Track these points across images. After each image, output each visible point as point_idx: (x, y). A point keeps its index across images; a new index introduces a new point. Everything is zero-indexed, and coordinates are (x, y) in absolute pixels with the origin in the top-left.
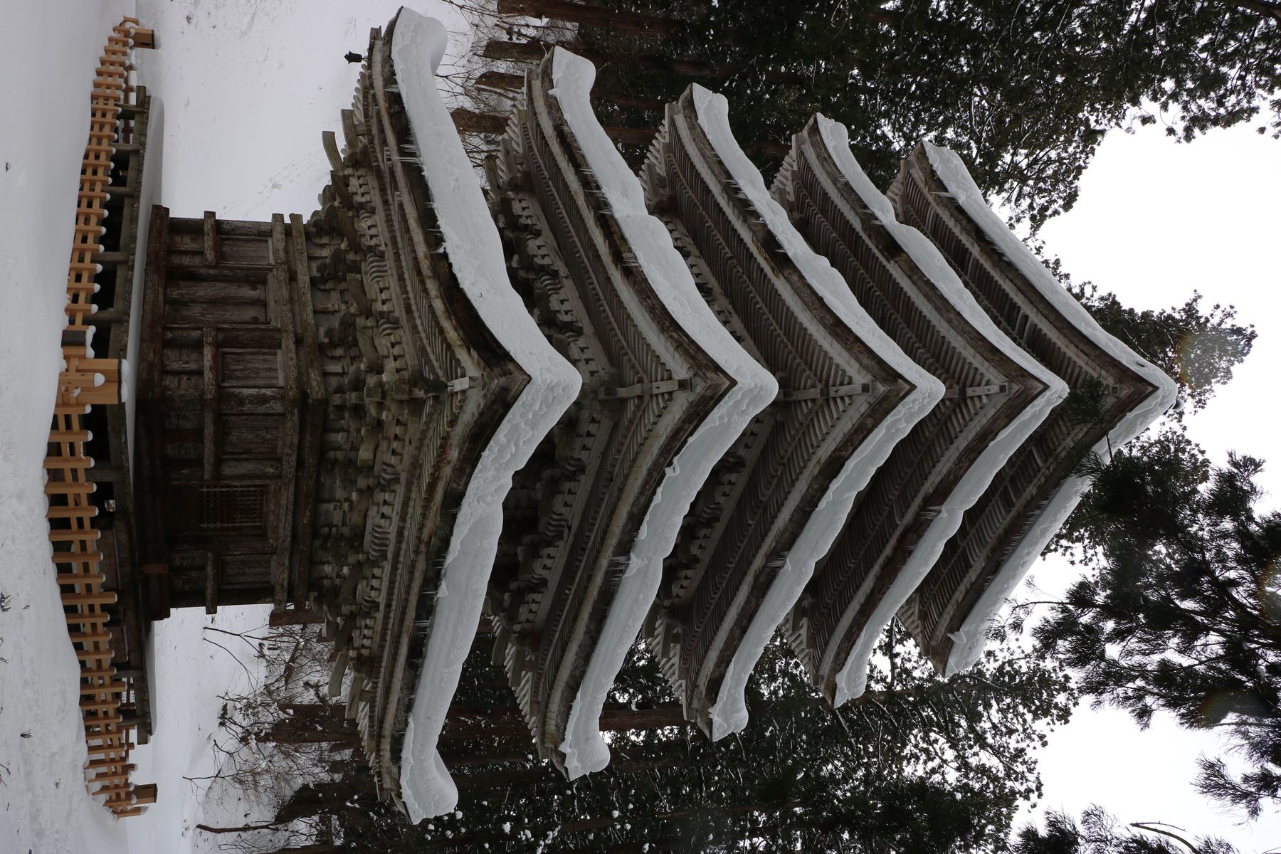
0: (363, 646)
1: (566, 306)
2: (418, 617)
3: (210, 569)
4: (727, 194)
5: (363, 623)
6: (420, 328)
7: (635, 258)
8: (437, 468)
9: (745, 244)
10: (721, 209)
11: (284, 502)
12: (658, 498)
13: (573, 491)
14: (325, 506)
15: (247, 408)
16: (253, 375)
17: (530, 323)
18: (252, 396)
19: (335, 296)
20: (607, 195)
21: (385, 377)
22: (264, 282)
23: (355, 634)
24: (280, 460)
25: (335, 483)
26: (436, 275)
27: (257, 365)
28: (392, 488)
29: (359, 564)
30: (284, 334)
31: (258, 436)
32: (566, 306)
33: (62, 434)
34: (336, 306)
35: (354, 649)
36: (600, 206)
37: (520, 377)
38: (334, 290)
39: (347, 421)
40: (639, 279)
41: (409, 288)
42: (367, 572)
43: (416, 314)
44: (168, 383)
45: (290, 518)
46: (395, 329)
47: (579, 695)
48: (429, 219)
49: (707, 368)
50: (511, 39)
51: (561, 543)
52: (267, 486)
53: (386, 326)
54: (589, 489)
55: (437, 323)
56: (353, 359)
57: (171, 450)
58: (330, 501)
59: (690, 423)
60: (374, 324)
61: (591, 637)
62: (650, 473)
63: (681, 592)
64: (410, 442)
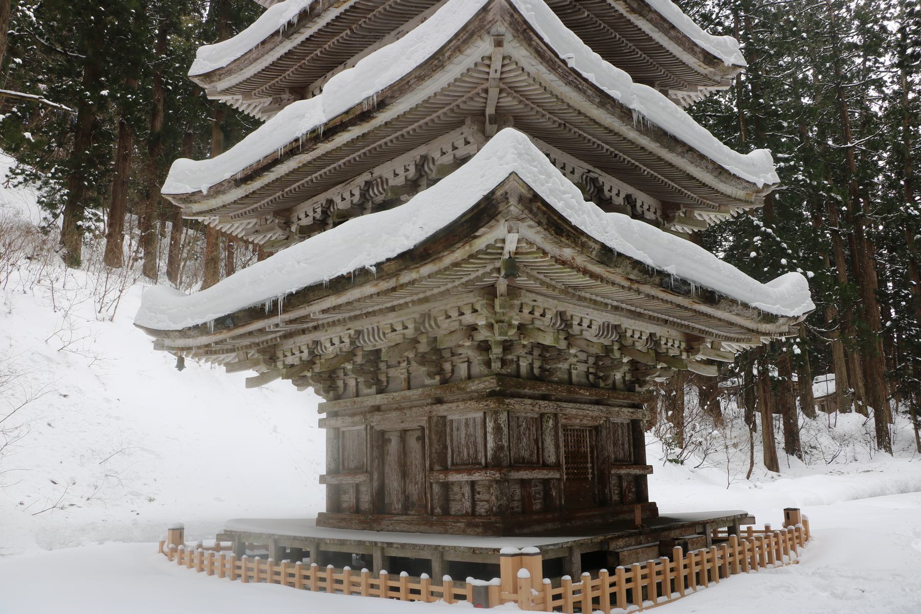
0: (679, 347)
1: (401, 172)
2: (687, 294)
3: (623, 472)
4: (293, 34)
5: (664, 346)
6: (443, 289)
7: (368, 98)
9: (341, 13)
10: (307, 39)
11: (574, 412)
12: (591, 77)
13: (562, 165)
14: (574, 378)
16: (472, 439)
17: (423, 197)
18: (495, 439)
19: (392, 372)
20: (304, 131)
21: (481, 322)
22: (383, 433)
23: (672, 353)
25: (560, 369)
26: (396, 274)
27: (463, 436)
28: (569, 318)
29: (622, 348)
30: (434, 413)
31: (524, 434)
32: (401, 172)
33: (566, 602)
34: (403, 371)
35: (681, 355)
36: (316, 136)
37: (512, 183)
38: (387, 374)
40: (389, 93)
41: (402, 301)
42: (629, 342)
43: (428, 293)
44: (483, 510)
45: (586, 406)
47: (726, 167)
48: (340, 284)
50: (141, 258)
51: (601, 180)
53: (427, 325)
54: (560, 151)
55: (446, 269)
57: (537, 506)
58: (570, 373)
59: (531, 39)
60: (424, 336)
61: (687, 151)
62: (569, 83)
64: (535, 301)
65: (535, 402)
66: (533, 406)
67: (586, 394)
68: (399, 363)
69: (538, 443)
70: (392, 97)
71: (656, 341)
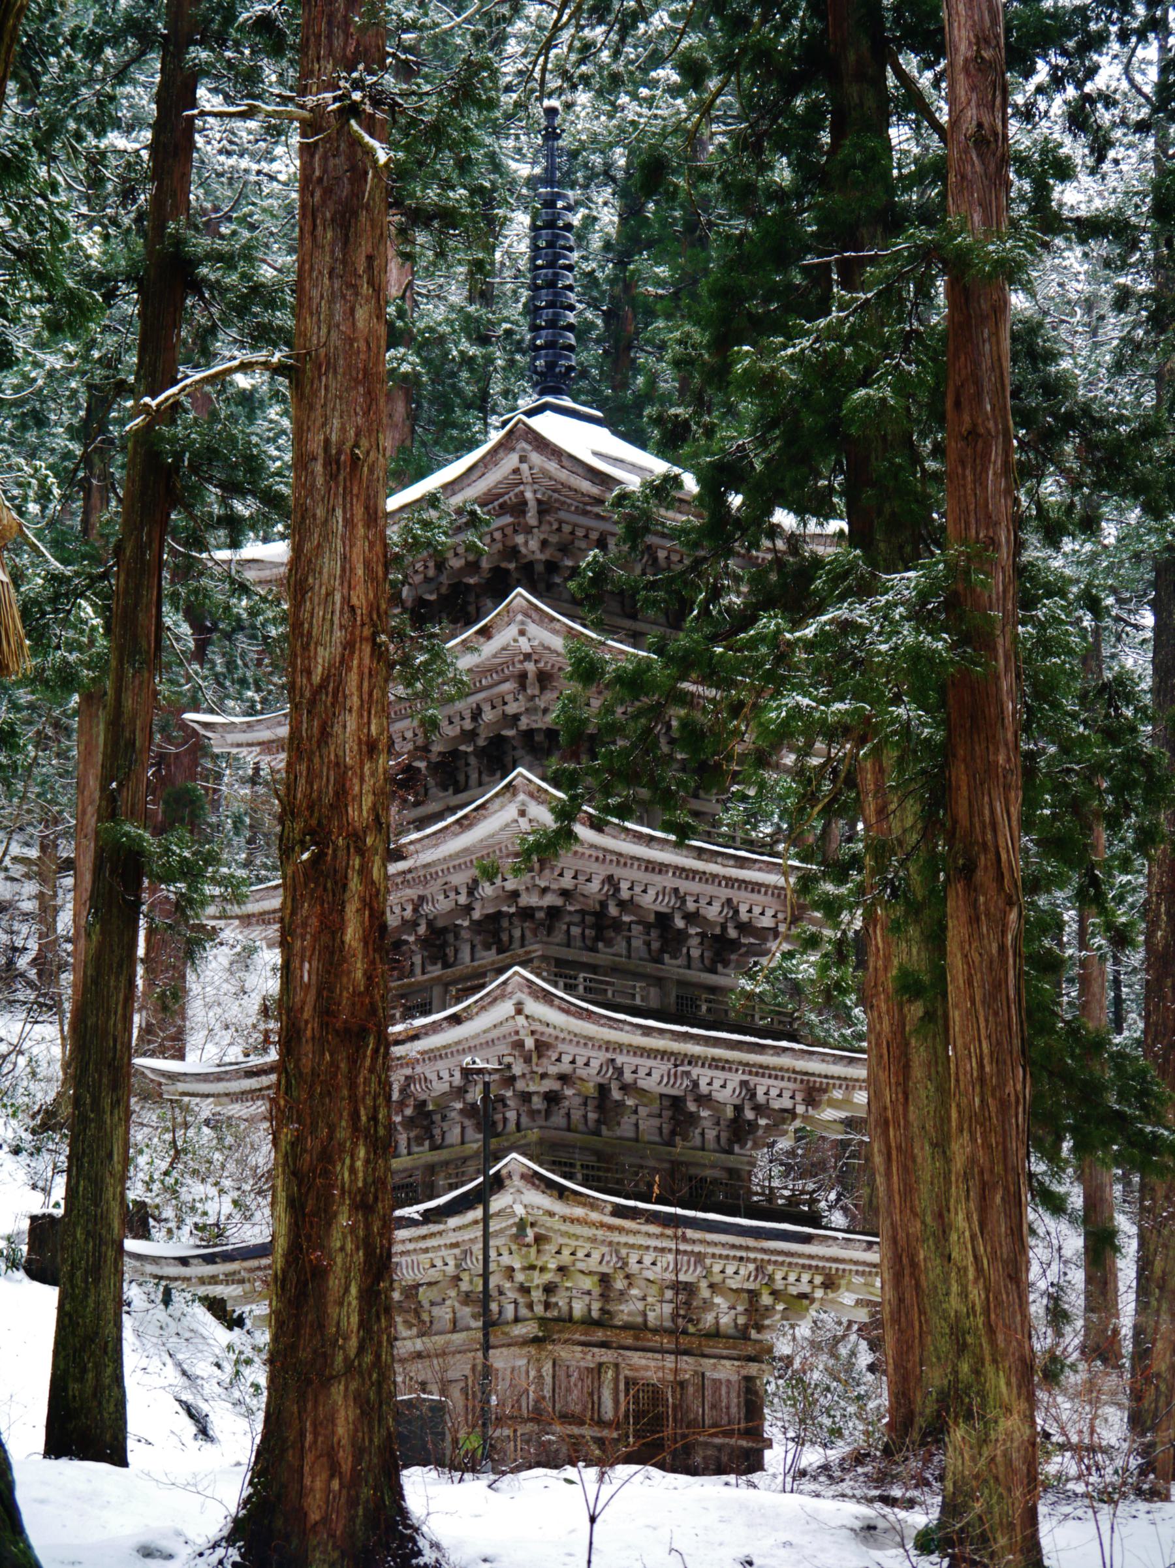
0: (810, 1282)
8: (593, 1224)
11: (643, 1362)
15: (547, 1393)
21: (517, 1266)
23: (794, 1291)
24: (600, 1365)
32: (445, 1075)
39: (560, 1299)
52: (626, 1378)
56: (501, 1293)
58: (645, 1315)
65: (586, 1349)
69: (593, 1395)
70: (426, 1034)
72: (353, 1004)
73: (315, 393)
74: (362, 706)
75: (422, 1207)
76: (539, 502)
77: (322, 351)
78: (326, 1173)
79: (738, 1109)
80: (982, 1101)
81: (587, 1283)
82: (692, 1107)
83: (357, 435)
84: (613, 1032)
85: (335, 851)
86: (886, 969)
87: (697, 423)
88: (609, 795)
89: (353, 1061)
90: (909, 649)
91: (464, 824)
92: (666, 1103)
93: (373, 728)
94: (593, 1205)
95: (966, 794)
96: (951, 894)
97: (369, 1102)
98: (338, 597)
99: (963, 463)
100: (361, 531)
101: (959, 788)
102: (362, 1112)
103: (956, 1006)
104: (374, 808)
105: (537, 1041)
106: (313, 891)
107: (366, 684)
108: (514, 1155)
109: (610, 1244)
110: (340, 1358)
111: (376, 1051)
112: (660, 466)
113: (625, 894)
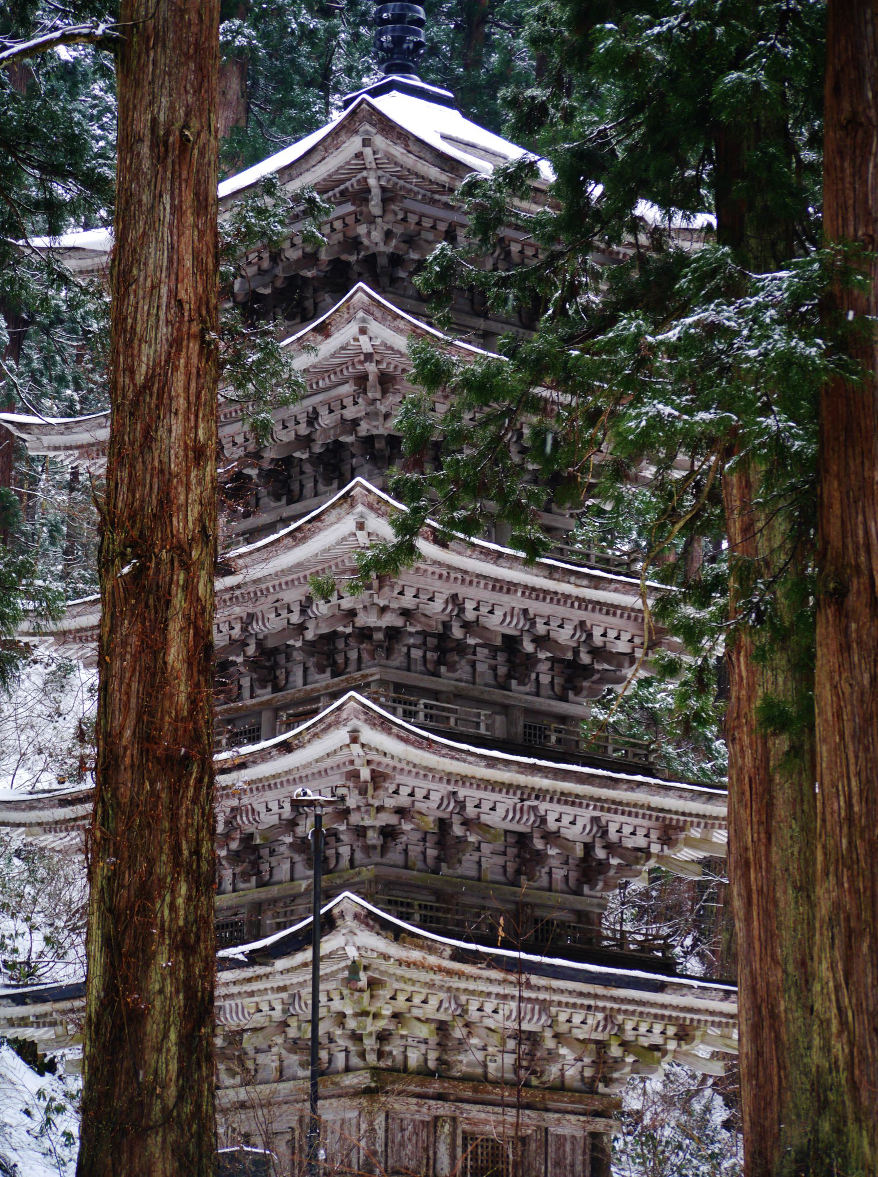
1: (274, 806)
11: (483, 1116)
13: (477, 802)
15: (380, 1149)
19: (262, 1059)
21: (349, 1011)
23: (645, 1042)
24: (437, 1118)
31: (409, 1139)
32: (274, 806)
38: (255, 1060)
39: (395, 1048)
46: (300, 998)
49: (338, 717)
52: (464, 1132)
53: (297, 1006)
56: (331, 1040)
58: (485, 1066)
63: (625, 637)
66: (420, 1106)
67: (508, 1095)
68: (270, 1047)
70: (254, 762)
71: (619, 1026)
72: (176, 729)
73: (142, 68)
74: (189, 408)
75: (247, 948)
76: (383, 189)
77: (151, 23)
78: (144, 911)
79: (588, 848)
80: (850, 843)
81: (424, 1031)
82: (538, 844)
83: (187, 114)
84: (455, 762)
85: (158, 564)
86: (749, 699)
87: (556, 107)
88: (453, 508)
89: (175, 792)
90: (780, 355)
91: (298, 537)
92: (511, 840)
93: (201, 432)
94: (431, 948)
95: (838, 512)
96: (821, 619)
97: (191, 834)
98: (164, 290)
99: (841, 154)
100: (190, 219)
101: (831, 506)
102: (184, 846)
103: (824, 741)
104: (200, 519)
105: (373, 771)
106: (134, 607)
107: (193, 385)
108: (347, 894)
109: (449, 989)
110: (157, 1107)
111: (199, 781)
112: (514, 152)
113: (470, 615)
